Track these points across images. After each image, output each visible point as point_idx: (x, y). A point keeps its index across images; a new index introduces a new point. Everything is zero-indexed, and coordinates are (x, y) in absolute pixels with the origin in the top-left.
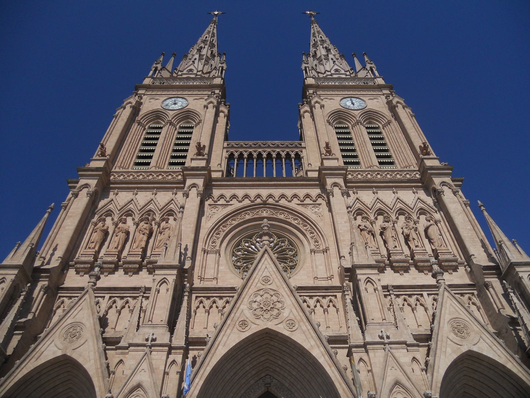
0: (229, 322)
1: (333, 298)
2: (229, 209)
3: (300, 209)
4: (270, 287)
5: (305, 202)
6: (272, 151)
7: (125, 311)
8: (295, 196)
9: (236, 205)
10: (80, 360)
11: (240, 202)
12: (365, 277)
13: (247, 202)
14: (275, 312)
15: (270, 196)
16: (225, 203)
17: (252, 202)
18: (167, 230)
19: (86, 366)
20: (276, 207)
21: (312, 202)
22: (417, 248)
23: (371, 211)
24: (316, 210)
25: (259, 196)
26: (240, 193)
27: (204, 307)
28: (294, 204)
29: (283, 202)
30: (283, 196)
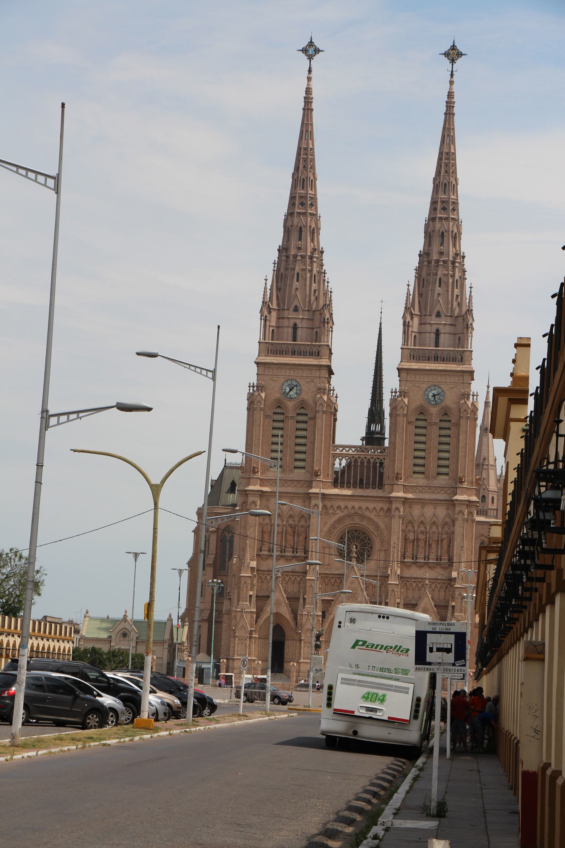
0: (337, 602)
1: (383, 581)
2: (336, 518)
3: (376, 519)
4: (353, 586)
5: (380, 514)
6: (365, 458)
7: (290, 583)
8: (375, 508)
9: (340, 514)
10: (284, 614)
11: (342, 512)
12: (391, 589)
13: (346, 512)
14: (355, 598)
15: (360, 508)
16: (333, 512)
17: (349, 512)
18: (303, 533)
19: (286, 616)
20: (362, 517)
21: (383, 514)
22: (432, 555)
23: (416, 523)
24: (386, 520)
25: (353, 507)
26: (342, 504)
27: (325, 582)
28: (372, 516)
29: (367, 513)
30: (367, 508)
